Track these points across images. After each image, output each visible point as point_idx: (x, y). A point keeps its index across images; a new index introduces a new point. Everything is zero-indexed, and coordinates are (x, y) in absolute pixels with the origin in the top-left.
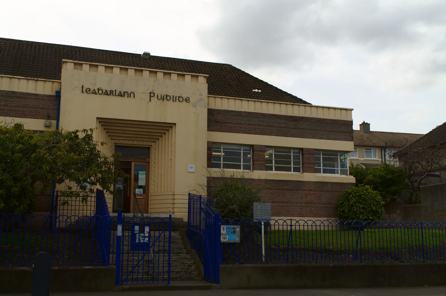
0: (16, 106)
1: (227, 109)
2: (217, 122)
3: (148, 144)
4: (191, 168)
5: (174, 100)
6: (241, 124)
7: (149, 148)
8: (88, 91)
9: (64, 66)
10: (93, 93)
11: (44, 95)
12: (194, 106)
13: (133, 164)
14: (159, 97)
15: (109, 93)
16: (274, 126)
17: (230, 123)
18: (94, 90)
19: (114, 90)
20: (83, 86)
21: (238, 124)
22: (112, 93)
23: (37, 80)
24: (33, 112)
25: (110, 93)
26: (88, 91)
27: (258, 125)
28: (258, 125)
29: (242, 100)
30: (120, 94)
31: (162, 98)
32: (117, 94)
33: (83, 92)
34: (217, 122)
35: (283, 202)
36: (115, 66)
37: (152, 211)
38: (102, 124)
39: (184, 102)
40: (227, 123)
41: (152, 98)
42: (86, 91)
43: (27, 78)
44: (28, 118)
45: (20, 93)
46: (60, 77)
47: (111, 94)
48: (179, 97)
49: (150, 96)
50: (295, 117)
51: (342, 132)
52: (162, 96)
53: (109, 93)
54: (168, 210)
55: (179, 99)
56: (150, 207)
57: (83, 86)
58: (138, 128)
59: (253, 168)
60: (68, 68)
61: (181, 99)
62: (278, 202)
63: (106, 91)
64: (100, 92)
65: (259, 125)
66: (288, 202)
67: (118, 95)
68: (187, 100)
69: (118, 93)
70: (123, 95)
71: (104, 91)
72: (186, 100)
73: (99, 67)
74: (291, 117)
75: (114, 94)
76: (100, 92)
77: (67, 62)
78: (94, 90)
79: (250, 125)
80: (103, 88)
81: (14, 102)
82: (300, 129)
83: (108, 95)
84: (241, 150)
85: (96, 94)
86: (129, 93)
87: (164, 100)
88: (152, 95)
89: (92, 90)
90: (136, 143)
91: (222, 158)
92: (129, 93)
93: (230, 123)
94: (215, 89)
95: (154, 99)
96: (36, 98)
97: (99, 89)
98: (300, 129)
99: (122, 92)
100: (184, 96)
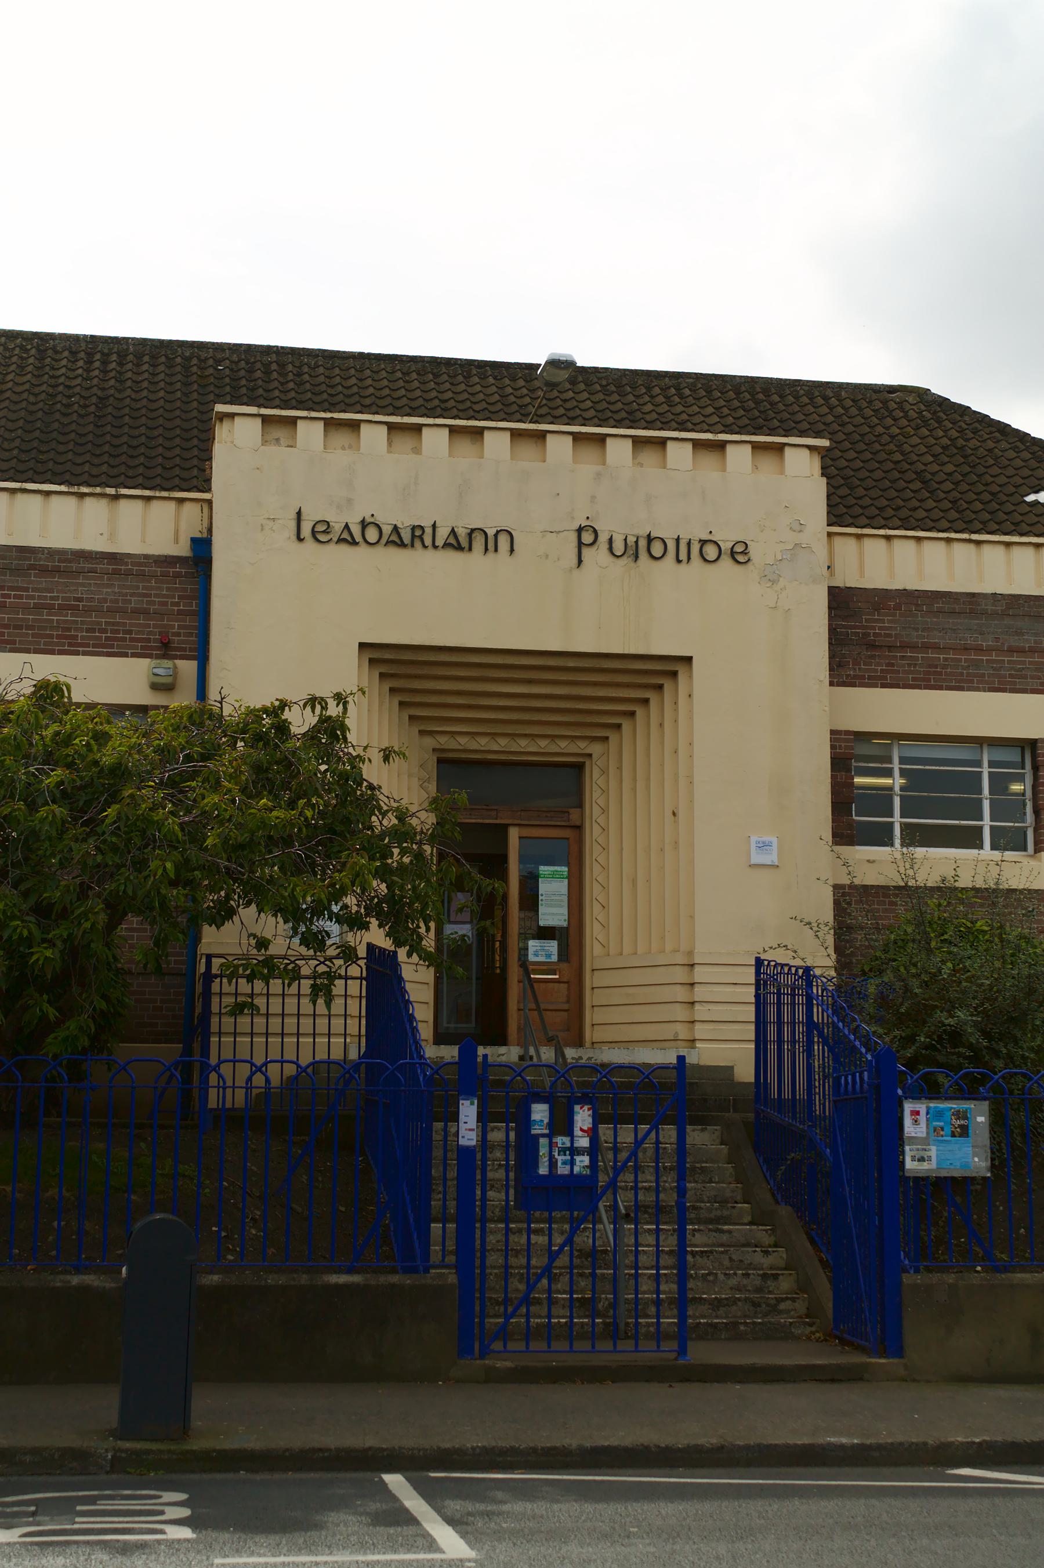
0: (37, 606)
1: (912, 586)
2: (872, 646)
3: (573, 748)
4: (763, 846)
5: (683, 556)
6: (979, 649)
7: (579, 767)
8: (321, 533)
9: (222, 432)
10: (340, 540)
11: (146, 557)
13: (514, 834)
14: (619, 547)
15: (406, 537)
17: (926, 647)
18: (347, 526)
19: (427, 524)
20: (299, 513)
21: (966, 649)
22: (421, 538)
23: (116, 497)
24: (104, 631)
25: (413, 536)
26: (321, 533)
29: (978, 543)
30: (452, 540)
31: (631, 552)
32: (440, 542)
33: (300, 539)
34: (872, 646)
36: (430, 421)
37: (599, 1035)
38: (384, 669)
39: (726, 562)
40: (914, 647)
41: (585, 551)
42: (314, 533)
43: (75, 489)
44: (85, 654)
45: (52, 553)
46: (209, 480)
47: (418, 543)
48: (703, 542)
49: (580, 544)
52: (631, 540)
53: (406, 537)
54: (666, 1032)
55: (703, 550)
56: (589, 1017)
57: (299, 513)
58: (530, 682)
59: (1036, 843)
60: (239, 440)
61: (711, 552)
63: (396, 528)
64: (372, 535)
67: (447, 545)
68: (739, 554)
69: (442, 534)
70: (464, 543)
71: (387, 530)
72: (733, 554)
73: (364, 427)
75: (428, 541)
76: (372, 535)
77: (232, 416)
78: (347, 526)
79: (1021, 651)
80: (380, 519)
81: (26, 589)
83: (402, 545)
84: (978, 763)
85: (354, 543)
86: (491, 532)
87: (636, 557)
88: (585, 537)
89: (337, 528)
90: (523, 745)
91: (897, 801)
92: (491, 532)
93: (926, 647)
94: (856, 502)
95: (597, 557)
96: (116, 572)
97: (364, 525)
99: (462, 533)
100: (726, 538)
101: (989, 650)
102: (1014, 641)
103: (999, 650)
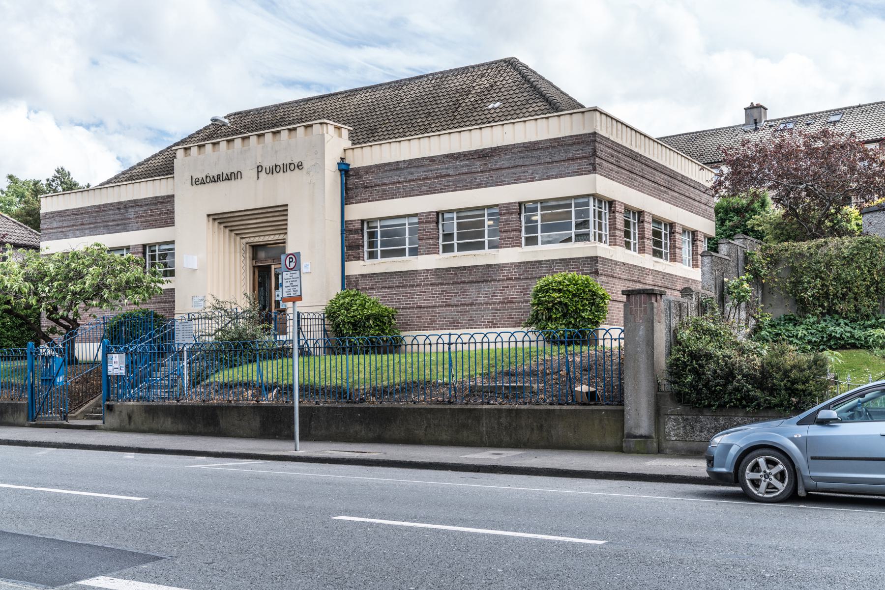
2: (366, 187)
6: (399, 182)
12: (308, 173)
13: (273, 267)
16: (448, 175)
17: (383, 184)
21: (395, 183)
27: (424, 179)
28: (424, 179)
34: (366, 187)
35: (463, 305)
40: (379, 185)
50: (484, 150)
51: (573, 159)
62: (456, 306)
65: (426, 179)
66: (471, 304)
68: (300, 166)
74: (476, 152)
79: (413, 181)
82: (493, 170)
93: (383, 184)
95: (263, 174)
98: (493, 170)
100: (296, 162)
101: (403, 182)
102: (410, 177)
103: (406, 182)
